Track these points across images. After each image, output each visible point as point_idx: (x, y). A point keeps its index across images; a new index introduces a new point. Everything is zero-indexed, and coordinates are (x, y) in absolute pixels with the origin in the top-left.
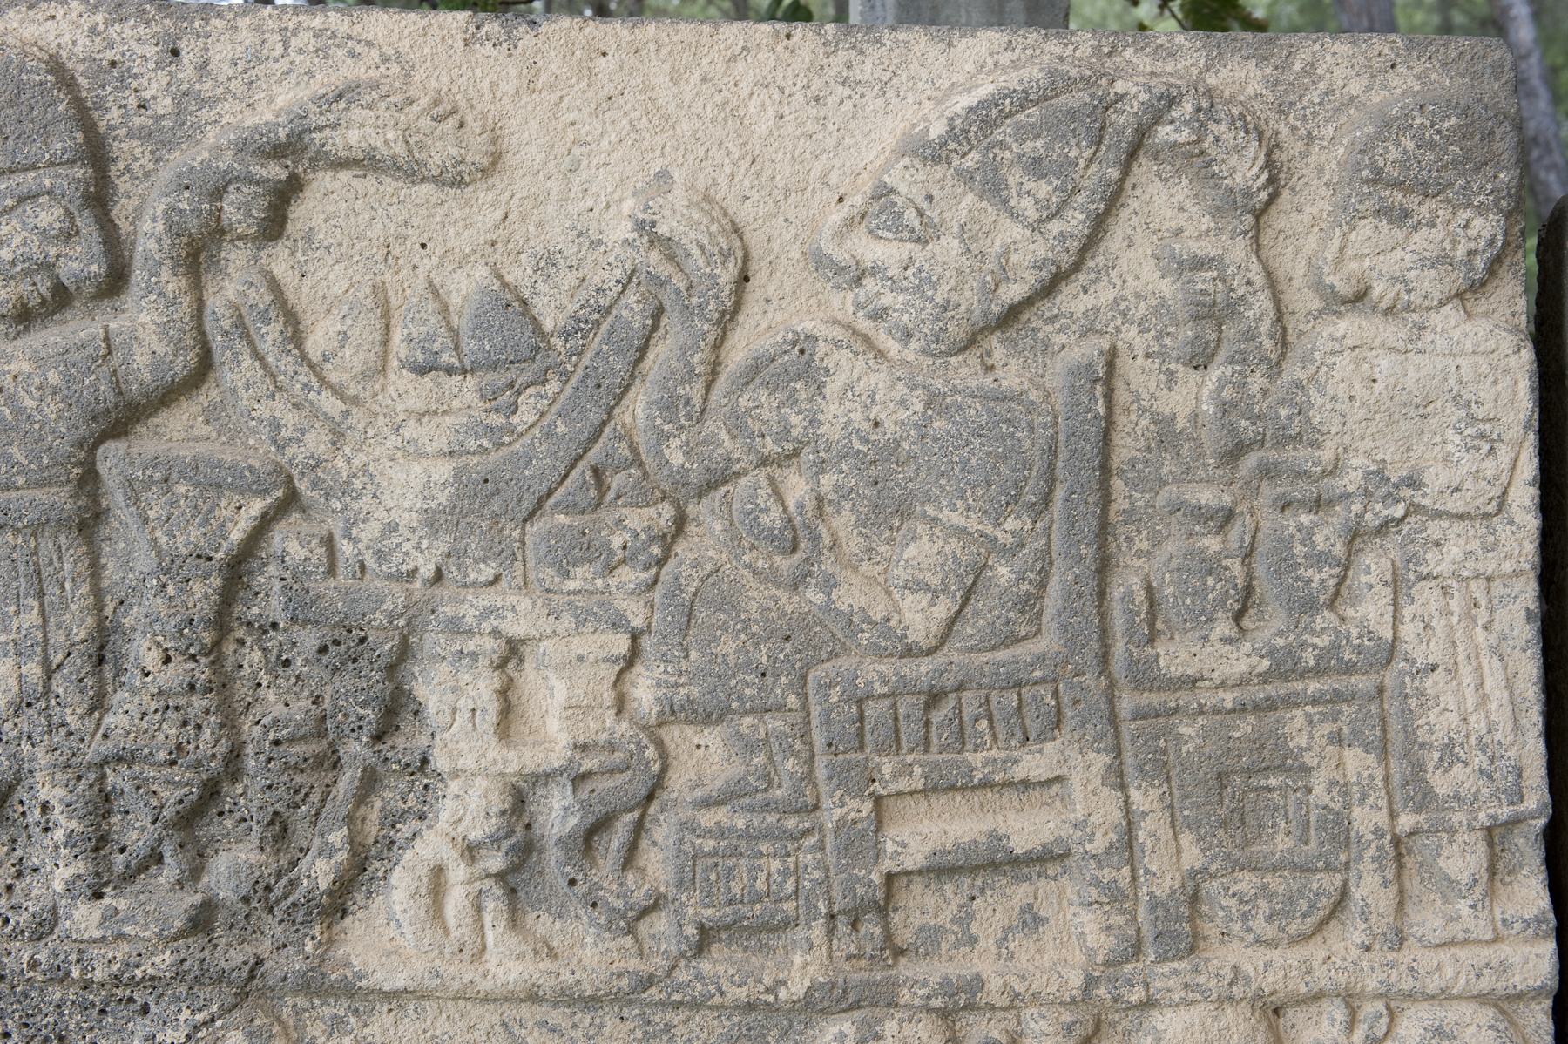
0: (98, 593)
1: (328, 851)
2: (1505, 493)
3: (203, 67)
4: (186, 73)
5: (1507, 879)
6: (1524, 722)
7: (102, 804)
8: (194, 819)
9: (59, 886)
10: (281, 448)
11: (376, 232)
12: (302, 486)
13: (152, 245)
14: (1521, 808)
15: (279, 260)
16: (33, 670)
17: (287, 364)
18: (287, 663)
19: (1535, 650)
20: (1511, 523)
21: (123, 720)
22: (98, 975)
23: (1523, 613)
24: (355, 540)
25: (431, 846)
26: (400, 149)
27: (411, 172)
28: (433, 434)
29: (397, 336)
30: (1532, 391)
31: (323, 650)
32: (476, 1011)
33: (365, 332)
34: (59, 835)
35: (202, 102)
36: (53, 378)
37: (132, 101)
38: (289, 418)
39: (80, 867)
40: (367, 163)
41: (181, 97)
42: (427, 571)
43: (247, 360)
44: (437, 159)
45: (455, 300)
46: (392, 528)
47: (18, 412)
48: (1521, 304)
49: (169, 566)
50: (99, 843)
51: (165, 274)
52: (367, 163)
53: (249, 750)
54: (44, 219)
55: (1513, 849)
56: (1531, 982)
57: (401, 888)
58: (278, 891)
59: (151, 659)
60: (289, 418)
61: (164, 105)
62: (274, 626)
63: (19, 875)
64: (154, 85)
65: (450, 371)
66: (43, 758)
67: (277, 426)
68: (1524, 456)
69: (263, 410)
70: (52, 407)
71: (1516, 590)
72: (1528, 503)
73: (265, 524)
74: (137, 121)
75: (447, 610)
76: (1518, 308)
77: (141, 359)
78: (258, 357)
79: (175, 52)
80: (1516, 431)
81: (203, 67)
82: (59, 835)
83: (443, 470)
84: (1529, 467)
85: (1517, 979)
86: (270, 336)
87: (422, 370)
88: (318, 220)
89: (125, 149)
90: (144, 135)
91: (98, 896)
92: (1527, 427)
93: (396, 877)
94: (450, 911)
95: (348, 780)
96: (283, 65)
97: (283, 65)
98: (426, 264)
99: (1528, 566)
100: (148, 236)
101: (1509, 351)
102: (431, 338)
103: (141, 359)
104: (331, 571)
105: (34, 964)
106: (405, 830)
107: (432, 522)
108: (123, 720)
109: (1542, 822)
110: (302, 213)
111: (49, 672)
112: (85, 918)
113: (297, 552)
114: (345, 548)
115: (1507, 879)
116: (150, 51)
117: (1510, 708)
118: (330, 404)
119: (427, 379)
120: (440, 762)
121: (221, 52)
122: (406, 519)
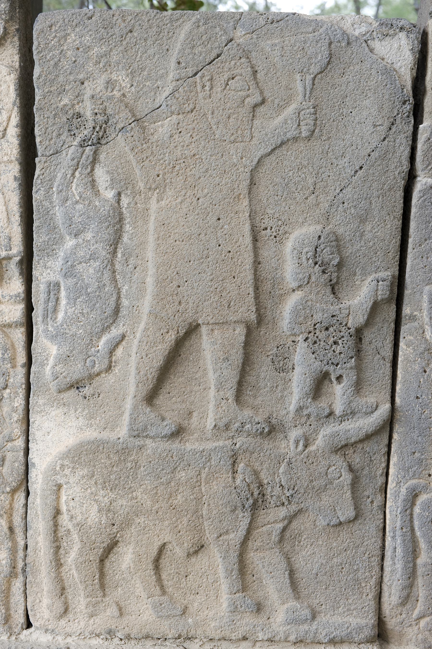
2: (5, 130)
5: (8, 281)
6: (13, 219)
14: (10, 252)
19: (17, 192)
20: (8, 142)
23: (13, 177)
30: (16, 90)
48: (17, 58)
55: (10, 270)
56: (12, 319)
68: (13, 116)
71: (10, 168)
72: (14, 134)
76: (15, 59)
80: (10, 106)
84: (15, 119)
85: (6, 318)
92: (14, 104)
99: (14, 159)
101: (6, 74)
109: (18, 258)
115: (8, 281)
117: (6, 213)
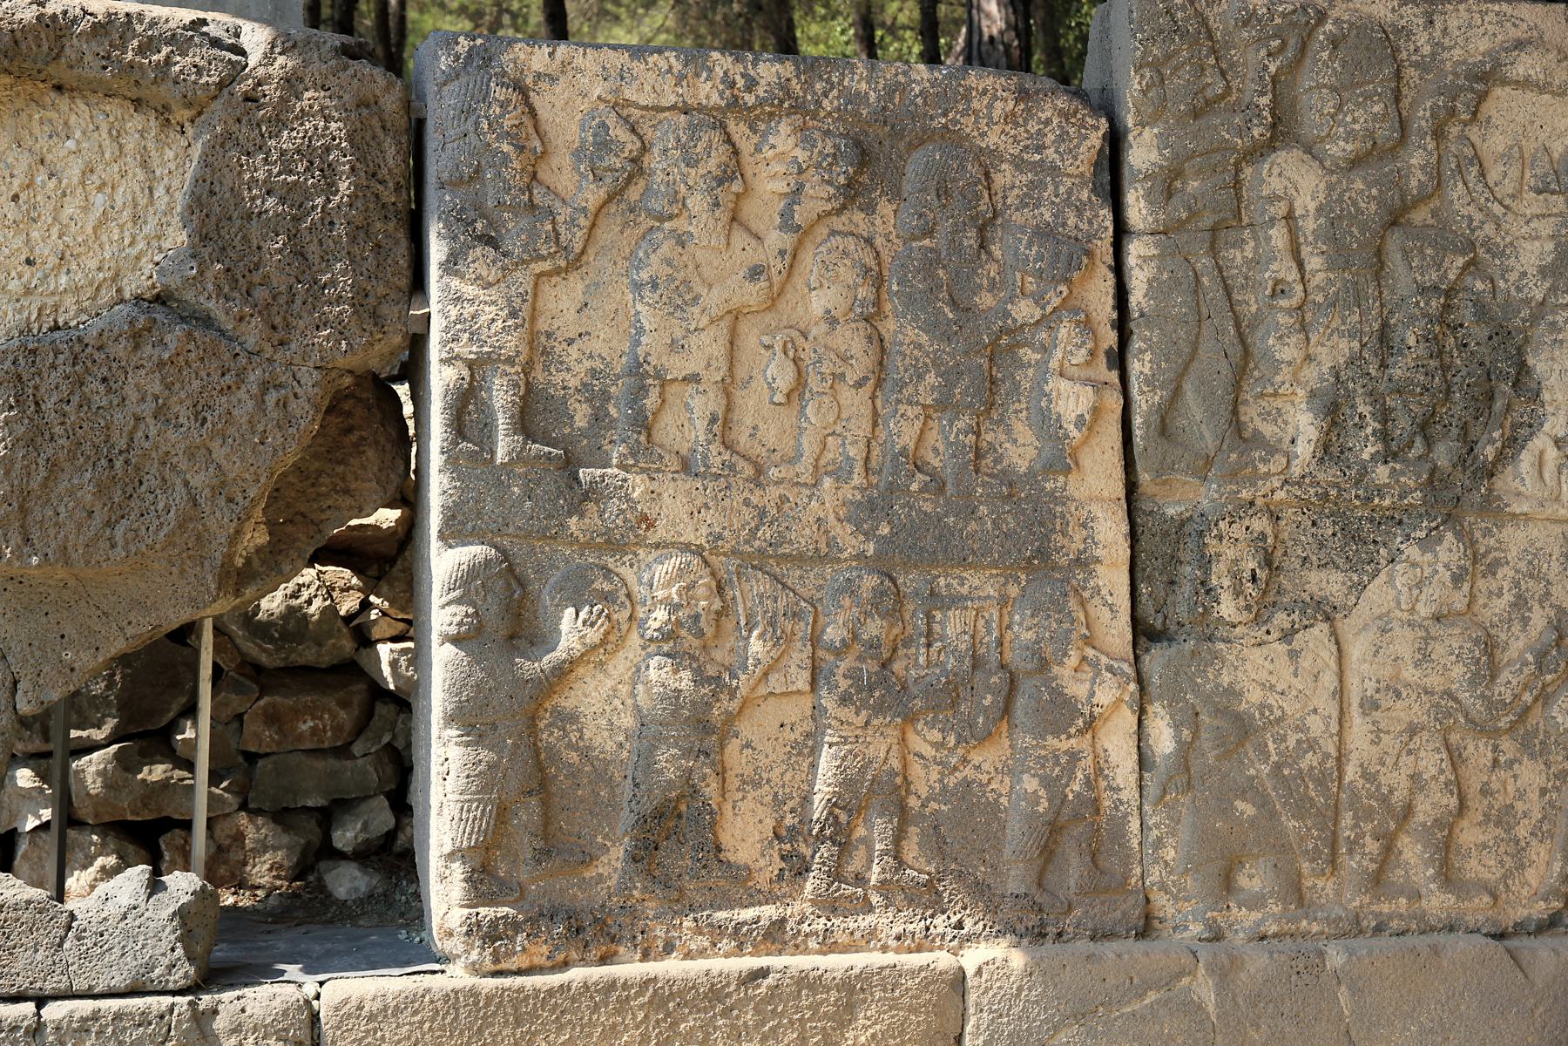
0: (1382, 305)
1: (1492, 441)
3: (1445, 31)
4: (1437, 34)
7: (1385, 416)
8: (1425, 428)
9: (1366, 456)
10: (1473, 231)
11: (1520, 119)
12: (1481, 251)
13: (1423, 123)
15: (1474, 133)
16: (1356, 345)
17: (1480, 187)
18: (1465, 345)
21: (1399, 372)
22: (1387, 502)
24: (1507, 281)
25: (1541, 442)
26: (1541, 76)
27: (1542, 88)
28: (1546, 228)
29: (1528, 175)
31: (1490, 338)
32: (1551, 527)
33: (1514, 172)
34: (1369, 430)
35: (1444, 49)
36: (1374, 192)
37: (1412, 48)
38: (1478, 216)
39: (1379, 447)
40: (1525, 84)
41: (1437, 46)
42: (1539, 297)
43: (1460, 185)
44: (1557, 82)
45: (1556, 156)
46: (1524, 274)
47: (1358, 209)
49: (1423, 290)
50: (1384, 436)
51: (1428, 138)
52: (1525, 84)
53: (1455, 388)
54: (1376, 109)
57: (1526, 460)
58: (1469, 462)
59: (1412, 341)
60: (1478, 216)
61: (1427, 50)
62: (1461, 326)
63: (1342, 452)
64: (1422, 39)
65: (1553, 192)
66: (1360, 391)
67: (1471, 219)
69: (1464, 212)
70: (1373, 207)
73: (1465, 268)
74: (1414, 58)
75: (1551, 318)
77: (1414, 183)
78: (1465, 184)
79: (1431, 22)
81: (1445, 31)
82: (1369, 430)
83: (1550, 246)
86: (1474, 170)
87: (1539, 192)
88: (1493, 113)
89: (1411, 73)
90: (1416, 65)
91: (1386, 462)
93: (1525, 455)
94: (1547, 476)
95: (1499, 405)
96: (1482, 30)
97: (1482, 30)
98: (1542, 136)
100: (1422, 118)
102: (1546, 175)
103: (1414, 183)
104: (1494, 297)
105: (1357, 497)
106: (1523, 432)
107: (1543, 271)
108: (1399, 372)
110: (1489, 108)
111: (1363, 346)
112: (1382, 473)
113: (1479, 286)
114: (1502, 284)
116: (1421, 22)
118: (1497, 209)
119: (1541, 197)
120: (1546, 396)
121: (1453, 23)
122: (1532, 271)
